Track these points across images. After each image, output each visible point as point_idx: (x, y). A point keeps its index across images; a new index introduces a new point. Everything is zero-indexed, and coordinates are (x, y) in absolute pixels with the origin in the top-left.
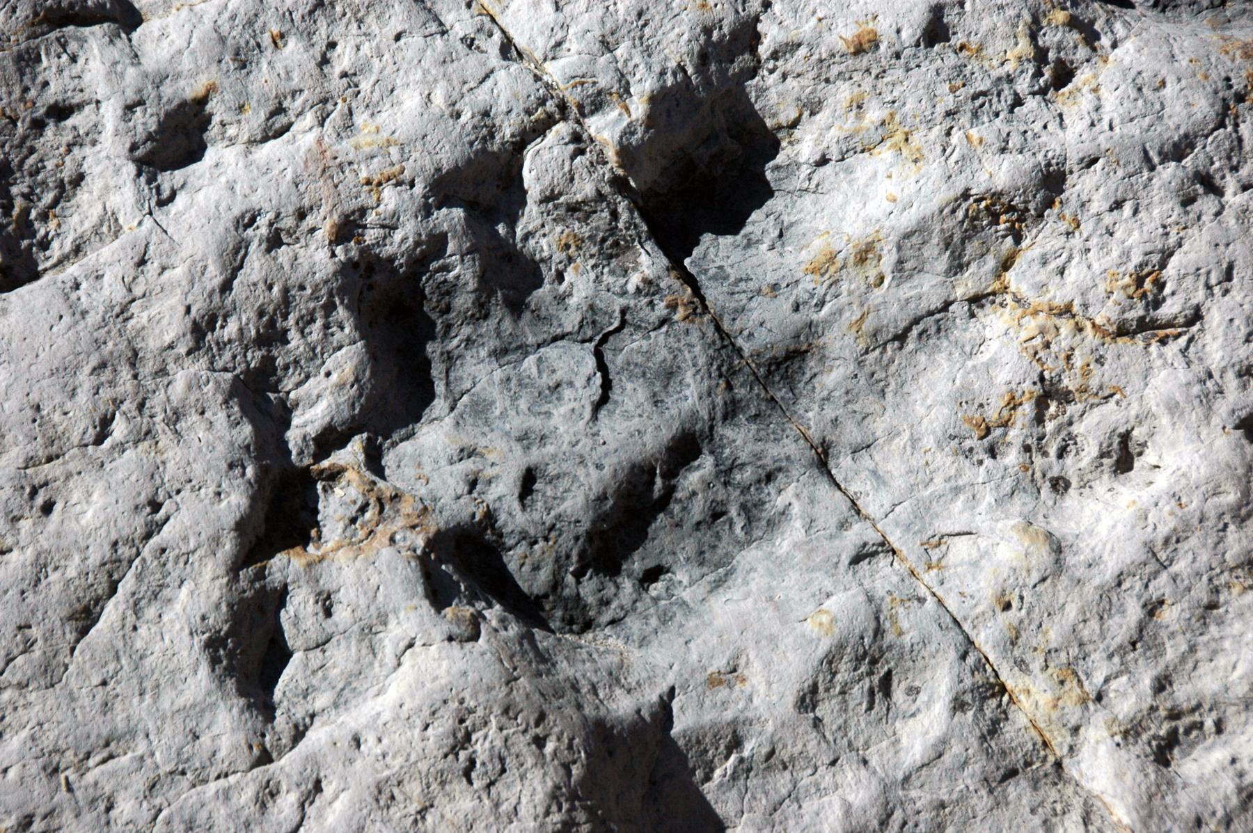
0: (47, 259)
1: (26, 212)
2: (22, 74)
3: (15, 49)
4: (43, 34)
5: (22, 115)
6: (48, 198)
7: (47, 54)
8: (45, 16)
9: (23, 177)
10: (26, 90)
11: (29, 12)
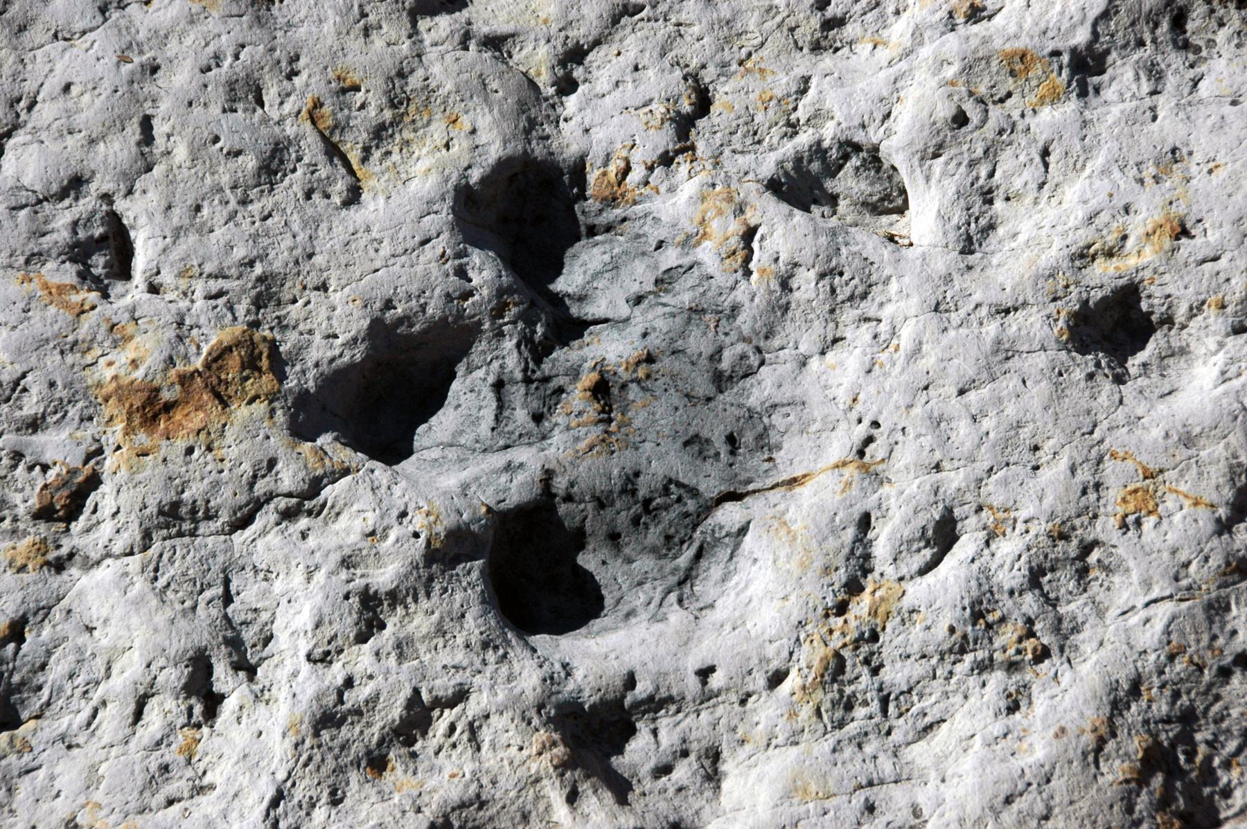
0: (1229, 807)
1: (1208, 759)
2: (1211, 622)
3: (1206, 597)
4: (1234, 583)
5: (1209, 662)
6: (1232, 746)
7: (1237, 603)
8: (1237, 566)
9: (1207, 724)
10: (1214, 638)
11: (1221, 562)
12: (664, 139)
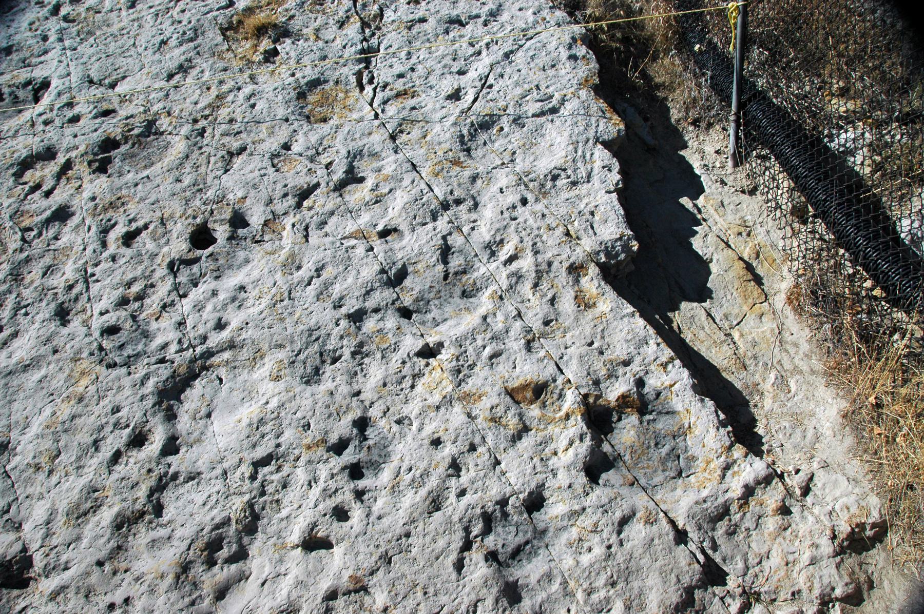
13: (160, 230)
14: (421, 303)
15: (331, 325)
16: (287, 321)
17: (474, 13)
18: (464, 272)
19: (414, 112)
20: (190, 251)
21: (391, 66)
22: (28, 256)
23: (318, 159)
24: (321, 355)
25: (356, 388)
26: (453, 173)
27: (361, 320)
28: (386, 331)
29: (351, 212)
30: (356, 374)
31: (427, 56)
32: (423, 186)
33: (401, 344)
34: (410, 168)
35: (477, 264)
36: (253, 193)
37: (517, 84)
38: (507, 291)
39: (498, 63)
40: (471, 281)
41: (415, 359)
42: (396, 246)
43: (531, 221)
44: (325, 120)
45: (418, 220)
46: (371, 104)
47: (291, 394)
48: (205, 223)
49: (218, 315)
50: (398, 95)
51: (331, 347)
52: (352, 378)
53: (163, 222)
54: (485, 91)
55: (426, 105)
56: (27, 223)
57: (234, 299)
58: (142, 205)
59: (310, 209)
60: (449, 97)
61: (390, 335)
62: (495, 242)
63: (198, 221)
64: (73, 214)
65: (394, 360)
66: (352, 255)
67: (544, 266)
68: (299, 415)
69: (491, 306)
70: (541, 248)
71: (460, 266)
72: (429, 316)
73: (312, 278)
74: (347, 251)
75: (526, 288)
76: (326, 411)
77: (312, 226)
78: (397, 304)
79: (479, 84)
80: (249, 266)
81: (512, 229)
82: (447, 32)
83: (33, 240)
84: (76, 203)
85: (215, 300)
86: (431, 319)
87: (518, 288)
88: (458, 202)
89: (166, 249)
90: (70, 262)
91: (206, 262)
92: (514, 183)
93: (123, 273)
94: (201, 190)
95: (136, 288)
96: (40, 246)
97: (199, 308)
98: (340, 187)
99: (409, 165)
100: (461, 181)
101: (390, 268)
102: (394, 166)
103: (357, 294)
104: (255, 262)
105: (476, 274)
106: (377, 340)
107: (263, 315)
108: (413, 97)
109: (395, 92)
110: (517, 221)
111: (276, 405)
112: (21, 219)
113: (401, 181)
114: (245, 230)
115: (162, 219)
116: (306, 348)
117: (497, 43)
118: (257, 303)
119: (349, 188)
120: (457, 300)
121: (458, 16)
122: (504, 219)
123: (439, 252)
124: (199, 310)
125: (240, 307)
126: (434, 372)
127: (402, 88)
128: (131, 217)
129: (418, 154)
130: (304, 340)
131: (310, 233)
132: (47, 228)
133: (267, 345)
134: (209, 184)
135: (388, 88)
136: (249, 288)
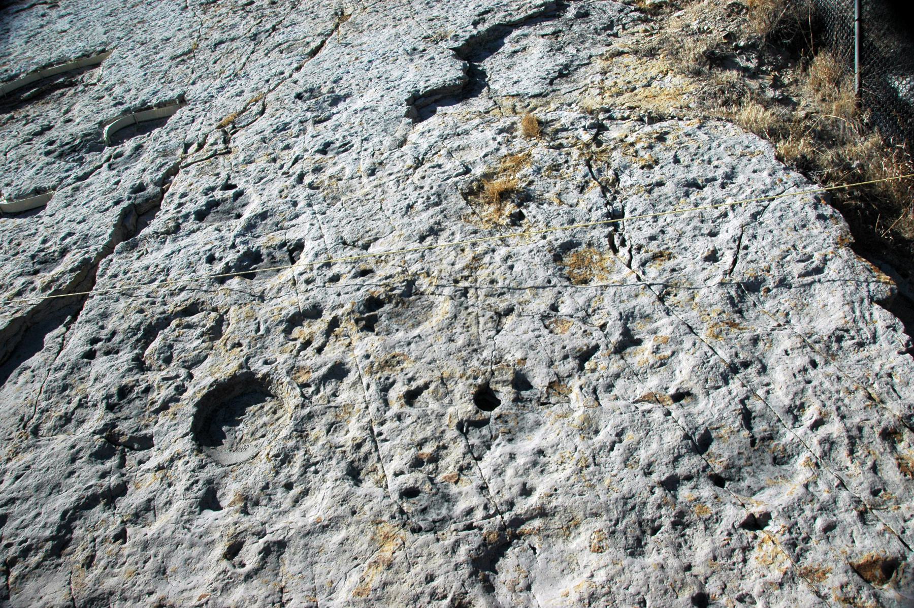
12: (721, 591)
13: (442, 390)
14: (733, 470)
15: (646, 493)
16: (598, 487)
17: (710, 176)
18: (771, 438)
19: (675, 274)
20: (477, 412)
21: (639, 229)
22: (310, 412)
23: (589, 320)
24: (640, 525)
25: (685, 561)
26: (731, 335)
27: (675, 489)
28: (703, 500)
29: (637, 375)
30: (680, 546)
31: (674, 218)
32: (707, 349)
33: (723, 514)
34: (688, 330)
35: (782, 431)
36: (531, 354)
37: (773, 245)
38: (822, 457)
39: (748, 224)
40: (781, 447)
41: (741, 531)
42: (694, 410)
43: (827, 385)
44: (585, 282)
45: (710, 384)
46: (629, 265)
47: (619, 567)
48: (487, 384)
49: (521, 480)
50: (655, 257)
51: (649, 517)
52: (678, 550)
53: (443, 381)
54: (742, 252)
55: (685, 267)
56: (303, 379)
57: (535, 464)
58: (418, 364)
59: (593, 371)
60: (707, 259)
61: (709, 505)
62: (796, 406)
63: (479, 381)
64: (349, 371)
65: (718, 531)
66: (650, 420)
67: (855, 432)
68: (632, 590)
69: (809, 474)
70: (847, 413)
71: (765, 431)
72: (744, 484)
73: (614, 443)
74: (644, 416)
75: (842, 453)
76: (660, 586)
77: (600, 389)
78: (708, 471)
79: (734, 246)
80: (542, 429)
81: (810, 392)
82: (687, 195)
83: (311, 396)
84: (349, 359)
85: (513, 464)
86: (746, 488)
87: (833, 455)
88: (746, 365)
89: (451, 410)
90: (353, 420)
91: (496, 424)
92: (799, 345)
93: (413, 433)
94: (475, 350)
95: (428, 449)
96: (320, 402)
97: (499, 471)
98: (620, 349)
99: (685, 327)
100: (743, 342)
101: (694, 433)
102: (671, 329)
103: (665, 460)
104: (548, 425)
105: (784, 441)
106: (696, 509)
107: (571, 481)
108: (669, 259)
109: (650, 254)
110: (813, 384)
111: (604, 578)
112: (298, 375)
113: (681, 344)
114: (528, 392)
115: (442, 379)
116: (624, 517)
117: (740, 205)
118: (561, 468)
119: (628, 350)
120: (769, 467)
121: (694, 179)
122: (799, 382)
123: (740, 417)
124: (500, 474)
125: (542, 472)
126: (765, 545)
127: (657, 250)
128: (410, 375)
129: (692, 316)
130: (620, 509)
131: (600, 397)
132: (324, 385)
133: (582, 513)
134: (483, 345)
135: (643, 251)
136: (549, 451)
